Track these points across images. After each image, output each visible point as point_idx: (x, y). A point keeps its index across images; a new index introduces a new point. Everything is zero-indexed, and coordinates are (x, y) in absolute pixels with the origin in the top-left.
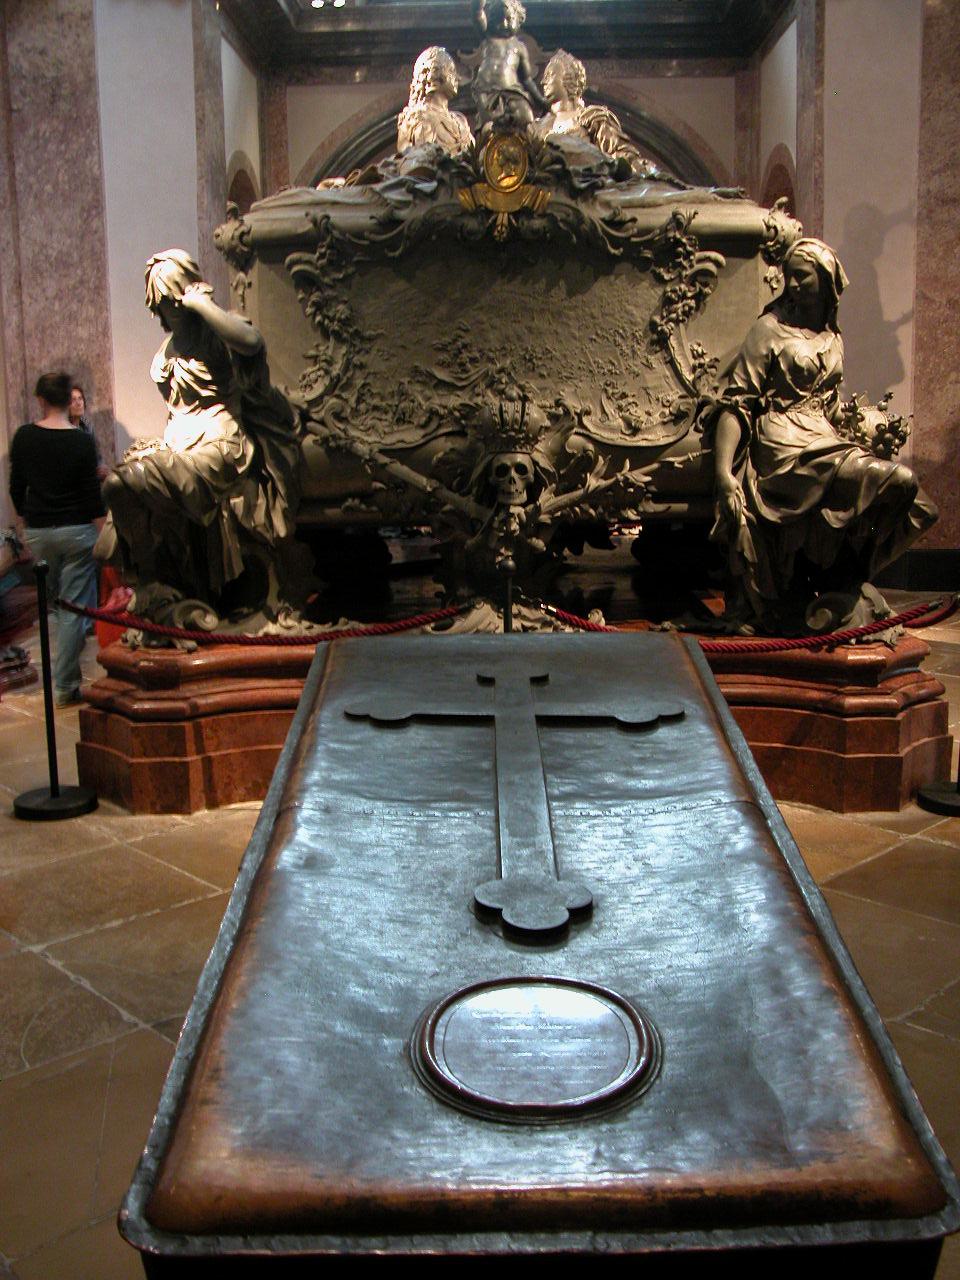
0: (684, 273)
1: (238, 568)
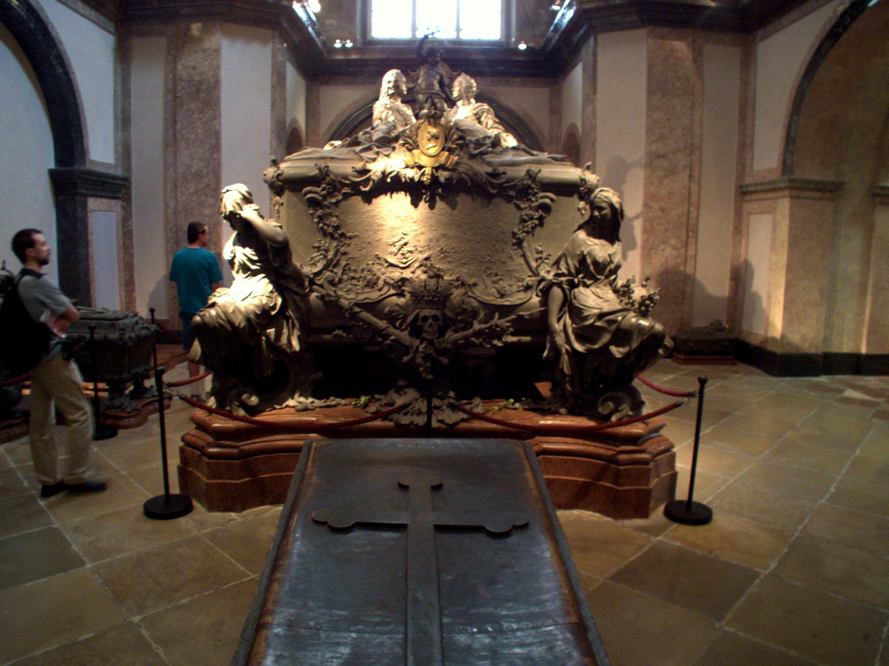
0: (533, 205)
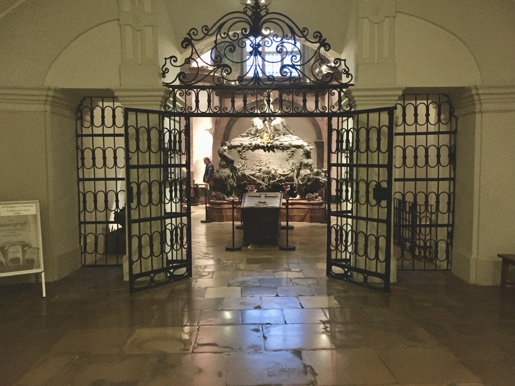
1: (229, 190)
